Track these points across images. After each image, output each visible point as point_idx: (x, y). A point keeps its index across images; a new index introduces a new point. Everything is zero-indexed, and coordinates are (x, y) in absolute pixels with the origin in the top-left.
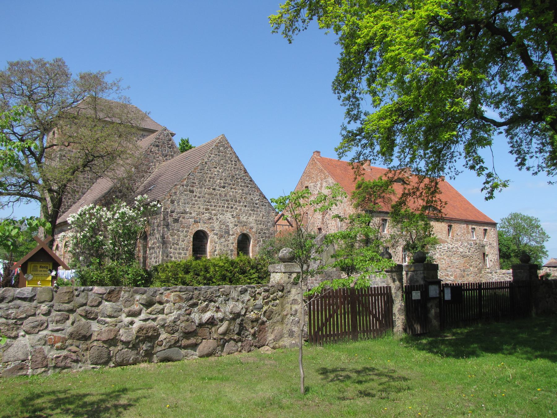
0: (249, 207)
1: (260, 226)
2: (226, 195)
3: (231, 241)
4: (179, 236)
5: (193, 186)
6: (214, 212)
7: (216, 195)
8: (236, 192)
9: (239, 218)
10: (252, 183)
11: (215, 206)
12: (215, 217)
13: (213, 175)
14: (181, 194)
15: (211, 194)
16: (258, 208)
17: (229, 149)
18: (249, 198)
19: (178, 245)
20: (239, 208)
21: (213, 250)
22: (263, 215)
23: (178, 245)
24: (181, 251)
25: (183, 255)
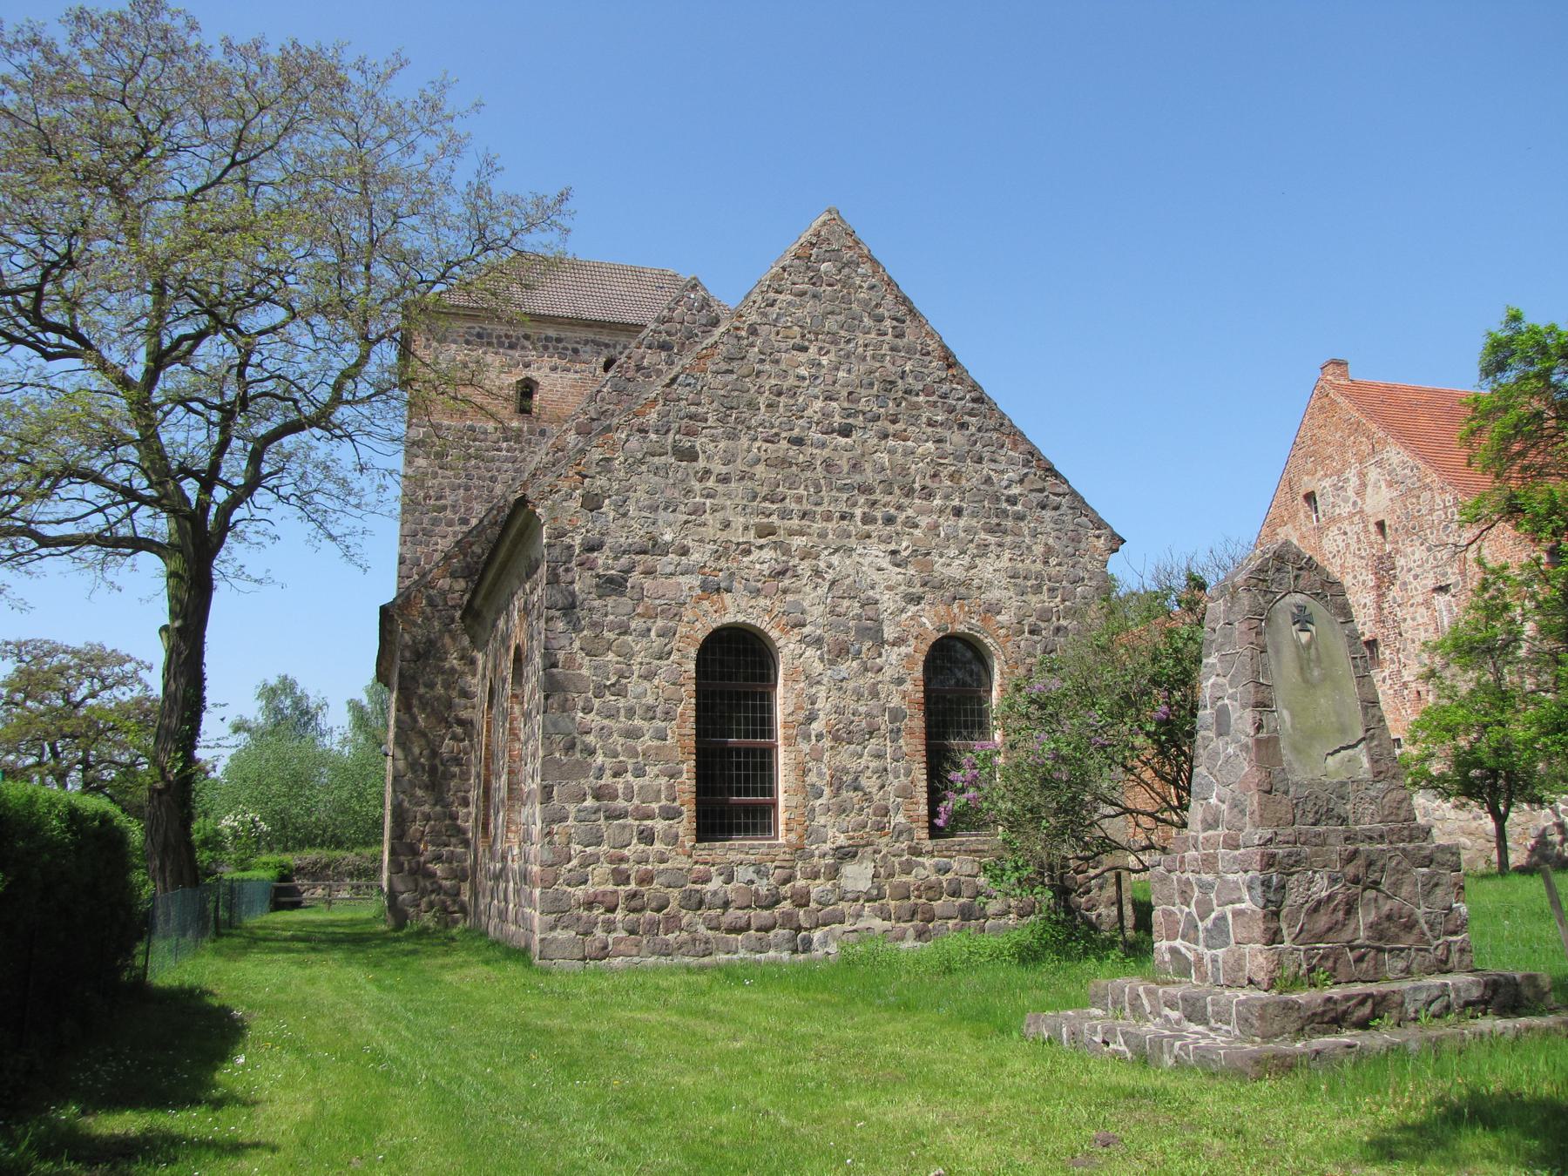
0: (974, 515)
1: (1033, 600)
2: (856, 467)
3: (888, 672)
4: (627, 655)
5: (691, 433)
6: (798, 541)
7: (810, 465)
8: (909, 453)
9: (928, 567)
10: (984, 408)
11: (804, 515)
12: (806, 564)
13: (791, 381)
14: (633, 465)
15: (785, 462)
16: (1020, 517)
17: (865, 269)
18: (973, 476)
19: (621, 693)
20: (924, 521)
21: (801, 716)
22: (1049, 551)
23: (621, 693)
24: (637, 722)
25: (647, 742)
